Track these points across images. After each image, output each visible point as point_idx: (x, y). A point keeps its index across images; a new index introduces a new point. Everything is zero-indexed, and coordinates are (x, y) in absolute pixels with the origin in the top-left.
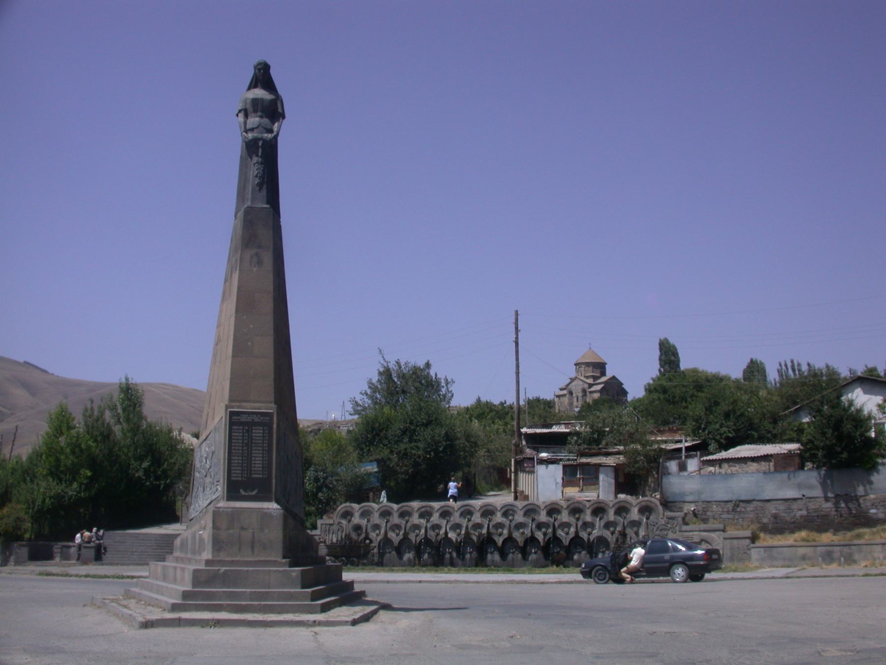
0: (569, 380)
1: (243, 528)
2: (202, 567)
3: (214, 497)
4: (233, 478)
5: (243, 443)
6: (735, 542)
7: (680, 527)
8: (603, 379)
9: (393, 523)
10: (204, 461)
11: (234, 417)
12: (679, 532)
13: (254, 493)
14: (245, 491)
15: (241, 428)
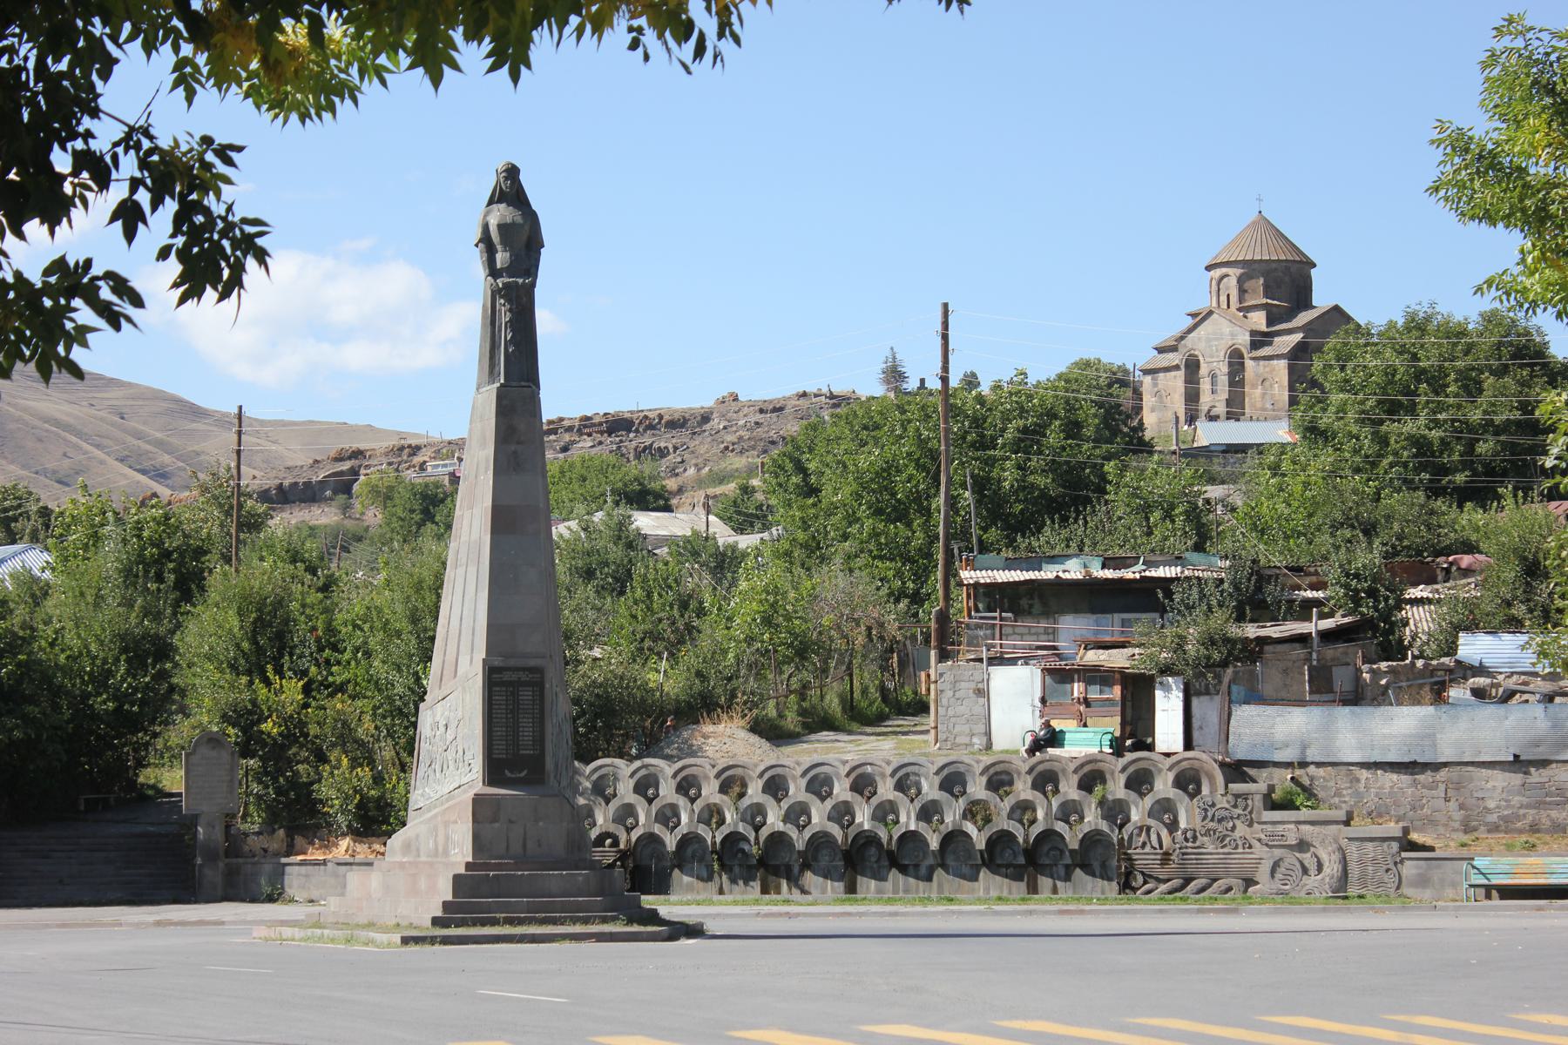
0: (1190, 322)
1: (511, 822)
2: (462, 870)
3: (465, 780)
4: (494, 756)
5: (507, 709)
6: (1370, 845)
7: (1259, 814)
8: (1304, 318)
9: (664, 803)
10: (442, 729)
11: (495, 676)
12: (1259, 823)
13: (523, 774)
14: (512, 772)
15: (504, 689)
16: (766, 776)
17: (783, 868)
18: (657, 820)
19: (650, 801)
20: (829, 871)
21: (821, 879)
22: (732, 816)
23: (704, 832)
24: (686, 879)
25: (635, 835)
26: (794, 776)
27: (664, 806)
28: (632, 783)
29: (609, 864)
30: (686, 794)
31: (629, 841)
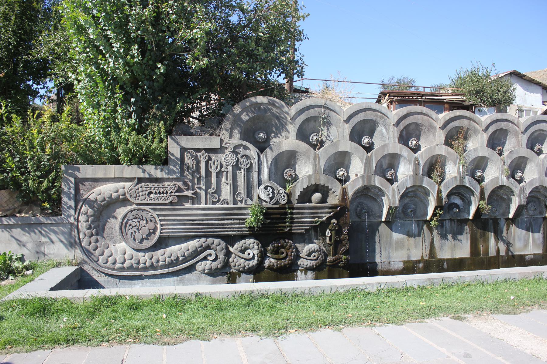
16: (491, 130)
17: (491, 222)
18: (376, 173)
19: (369, 148)
20: (531, 224)
21: (524, 232)
22: (459, 169)
23: (430, 185)
24: (396, 236)
25: (351, 188)
26: (516, 131)
27: (384, 157)
28: (347, 129)
29: (322, 222)
30: (406, 143)
31: (344, 193)
